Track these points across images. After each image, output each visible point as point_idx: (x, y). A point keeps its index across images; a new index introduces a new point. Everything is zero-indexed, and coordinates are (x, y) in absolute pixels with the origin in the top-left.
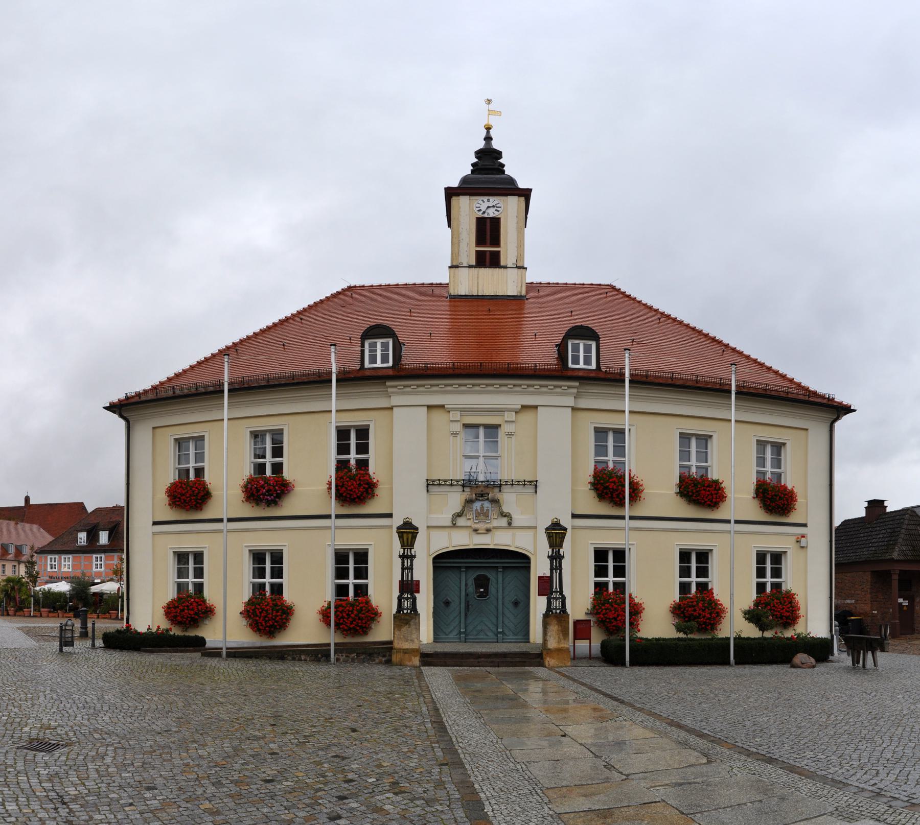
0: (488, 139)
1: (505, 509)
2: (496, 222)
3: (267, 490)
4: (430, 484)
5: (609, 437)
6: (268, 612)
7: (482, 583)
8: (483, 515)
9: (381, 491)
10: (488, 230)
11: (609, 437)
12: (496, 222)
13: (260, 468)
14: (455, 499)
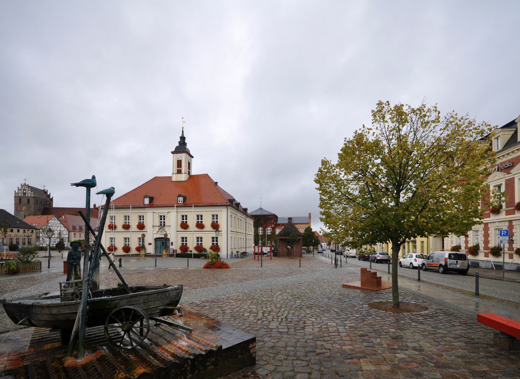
0: (183, 134)
2: (181, 161)
3: (126, 227)
4: (153, 226)
6: (127, 249)
12: (181, 161)
13: (126, 222)
14: (157, 229)
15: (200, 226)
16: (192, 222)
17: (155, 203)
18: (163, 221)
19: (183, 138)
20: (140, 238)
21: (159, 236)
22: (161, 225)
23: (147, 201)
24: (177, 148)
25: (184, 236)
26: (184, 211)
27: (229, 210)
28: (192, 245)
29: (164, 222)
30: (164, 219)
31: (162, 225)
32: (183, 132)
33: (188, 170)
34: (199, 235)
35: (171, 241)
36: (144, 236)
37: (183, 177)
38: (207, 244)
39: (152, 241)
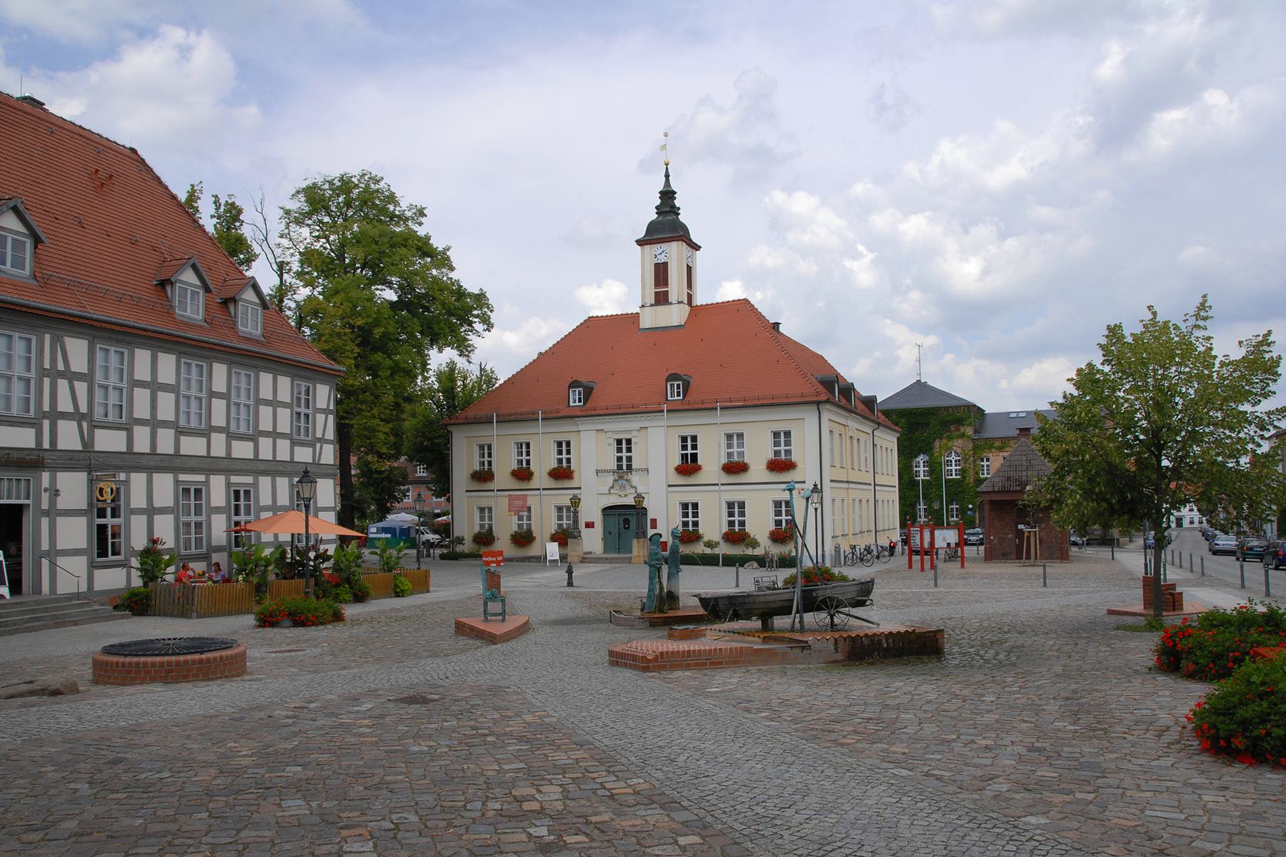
1: (634, 484)
2: (665, 264)
3: (523, 474)
5: (688, 442)
7: (627, 521)
8: (623, 487)
9: (576, 475)
10: (661, 273)
11: (688, 442)
12: (665, 264)
14: (610, 479)
15: (735, 468)
16: (711, 456)
17: (597, 400)
18: (624, 454)
19: (668, 195)
20: (560, 509)
21: (614, 500)
22: (620, 467)
23: (574, 399)
24: (652, 228)
25: (690, 499)
26: (690, 424)
27: (826, 416)
28: (712, 526)
29: (629, 459)
30: (629, 450)
31: (624, 468)
32: (667, 176)
33: (686, 290)
34: (735, 495)
35: (650, 516)
36: (576, 502)
37: (674, 315)
38: (760, 524)
39: (598, 519)
